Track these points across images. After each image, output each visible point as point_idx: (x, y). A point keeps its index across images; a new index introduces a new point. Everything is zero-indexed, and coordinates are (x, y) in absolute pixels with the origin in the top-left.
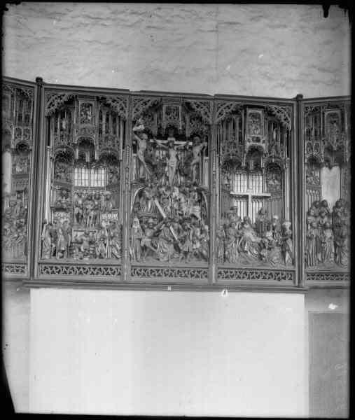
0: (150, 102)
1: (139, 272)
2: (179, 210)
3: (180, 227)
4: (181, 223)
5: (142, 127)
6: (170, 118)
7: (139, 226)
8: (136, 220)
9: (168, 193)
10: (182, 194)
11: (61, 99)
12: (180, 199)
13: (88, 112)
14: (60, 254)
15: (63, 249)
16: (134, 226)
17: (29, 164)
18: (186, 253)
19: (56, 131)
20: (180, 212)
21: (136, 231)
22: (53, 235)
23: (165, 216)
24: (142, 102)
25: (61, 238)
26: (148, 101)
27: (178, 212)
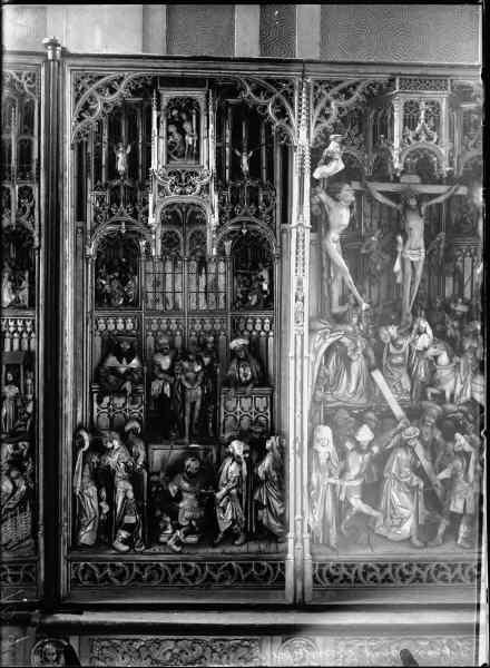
0: (359, 88)
1: (333, 572)
2: (431, 386)
3: (438, 435)
4: (439, 423)
5: (337, 166)
6: (417, 138)
7: (331, 448)
8: (325, 433)
9: (405, 343)
10: (441, 345)
11: (112, 91)
12: (436, 358)
13: (187, 126)
14: (124, 534)
15: (130, 519)
16: (317, 446)
17: (32, 282)
18: (455, 519)
19: (98, 177)
20: (435, 391)
21: (323, 461)
22: (104, 478)
23: (398, 411)
24: (335, 90)
25: (124, 489)
26: (354, 86)
27: (431, 391)
